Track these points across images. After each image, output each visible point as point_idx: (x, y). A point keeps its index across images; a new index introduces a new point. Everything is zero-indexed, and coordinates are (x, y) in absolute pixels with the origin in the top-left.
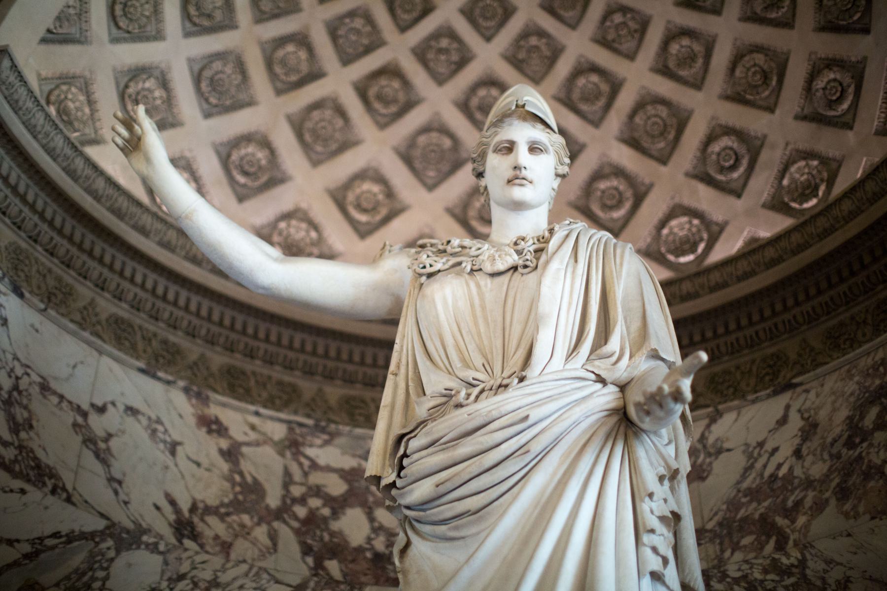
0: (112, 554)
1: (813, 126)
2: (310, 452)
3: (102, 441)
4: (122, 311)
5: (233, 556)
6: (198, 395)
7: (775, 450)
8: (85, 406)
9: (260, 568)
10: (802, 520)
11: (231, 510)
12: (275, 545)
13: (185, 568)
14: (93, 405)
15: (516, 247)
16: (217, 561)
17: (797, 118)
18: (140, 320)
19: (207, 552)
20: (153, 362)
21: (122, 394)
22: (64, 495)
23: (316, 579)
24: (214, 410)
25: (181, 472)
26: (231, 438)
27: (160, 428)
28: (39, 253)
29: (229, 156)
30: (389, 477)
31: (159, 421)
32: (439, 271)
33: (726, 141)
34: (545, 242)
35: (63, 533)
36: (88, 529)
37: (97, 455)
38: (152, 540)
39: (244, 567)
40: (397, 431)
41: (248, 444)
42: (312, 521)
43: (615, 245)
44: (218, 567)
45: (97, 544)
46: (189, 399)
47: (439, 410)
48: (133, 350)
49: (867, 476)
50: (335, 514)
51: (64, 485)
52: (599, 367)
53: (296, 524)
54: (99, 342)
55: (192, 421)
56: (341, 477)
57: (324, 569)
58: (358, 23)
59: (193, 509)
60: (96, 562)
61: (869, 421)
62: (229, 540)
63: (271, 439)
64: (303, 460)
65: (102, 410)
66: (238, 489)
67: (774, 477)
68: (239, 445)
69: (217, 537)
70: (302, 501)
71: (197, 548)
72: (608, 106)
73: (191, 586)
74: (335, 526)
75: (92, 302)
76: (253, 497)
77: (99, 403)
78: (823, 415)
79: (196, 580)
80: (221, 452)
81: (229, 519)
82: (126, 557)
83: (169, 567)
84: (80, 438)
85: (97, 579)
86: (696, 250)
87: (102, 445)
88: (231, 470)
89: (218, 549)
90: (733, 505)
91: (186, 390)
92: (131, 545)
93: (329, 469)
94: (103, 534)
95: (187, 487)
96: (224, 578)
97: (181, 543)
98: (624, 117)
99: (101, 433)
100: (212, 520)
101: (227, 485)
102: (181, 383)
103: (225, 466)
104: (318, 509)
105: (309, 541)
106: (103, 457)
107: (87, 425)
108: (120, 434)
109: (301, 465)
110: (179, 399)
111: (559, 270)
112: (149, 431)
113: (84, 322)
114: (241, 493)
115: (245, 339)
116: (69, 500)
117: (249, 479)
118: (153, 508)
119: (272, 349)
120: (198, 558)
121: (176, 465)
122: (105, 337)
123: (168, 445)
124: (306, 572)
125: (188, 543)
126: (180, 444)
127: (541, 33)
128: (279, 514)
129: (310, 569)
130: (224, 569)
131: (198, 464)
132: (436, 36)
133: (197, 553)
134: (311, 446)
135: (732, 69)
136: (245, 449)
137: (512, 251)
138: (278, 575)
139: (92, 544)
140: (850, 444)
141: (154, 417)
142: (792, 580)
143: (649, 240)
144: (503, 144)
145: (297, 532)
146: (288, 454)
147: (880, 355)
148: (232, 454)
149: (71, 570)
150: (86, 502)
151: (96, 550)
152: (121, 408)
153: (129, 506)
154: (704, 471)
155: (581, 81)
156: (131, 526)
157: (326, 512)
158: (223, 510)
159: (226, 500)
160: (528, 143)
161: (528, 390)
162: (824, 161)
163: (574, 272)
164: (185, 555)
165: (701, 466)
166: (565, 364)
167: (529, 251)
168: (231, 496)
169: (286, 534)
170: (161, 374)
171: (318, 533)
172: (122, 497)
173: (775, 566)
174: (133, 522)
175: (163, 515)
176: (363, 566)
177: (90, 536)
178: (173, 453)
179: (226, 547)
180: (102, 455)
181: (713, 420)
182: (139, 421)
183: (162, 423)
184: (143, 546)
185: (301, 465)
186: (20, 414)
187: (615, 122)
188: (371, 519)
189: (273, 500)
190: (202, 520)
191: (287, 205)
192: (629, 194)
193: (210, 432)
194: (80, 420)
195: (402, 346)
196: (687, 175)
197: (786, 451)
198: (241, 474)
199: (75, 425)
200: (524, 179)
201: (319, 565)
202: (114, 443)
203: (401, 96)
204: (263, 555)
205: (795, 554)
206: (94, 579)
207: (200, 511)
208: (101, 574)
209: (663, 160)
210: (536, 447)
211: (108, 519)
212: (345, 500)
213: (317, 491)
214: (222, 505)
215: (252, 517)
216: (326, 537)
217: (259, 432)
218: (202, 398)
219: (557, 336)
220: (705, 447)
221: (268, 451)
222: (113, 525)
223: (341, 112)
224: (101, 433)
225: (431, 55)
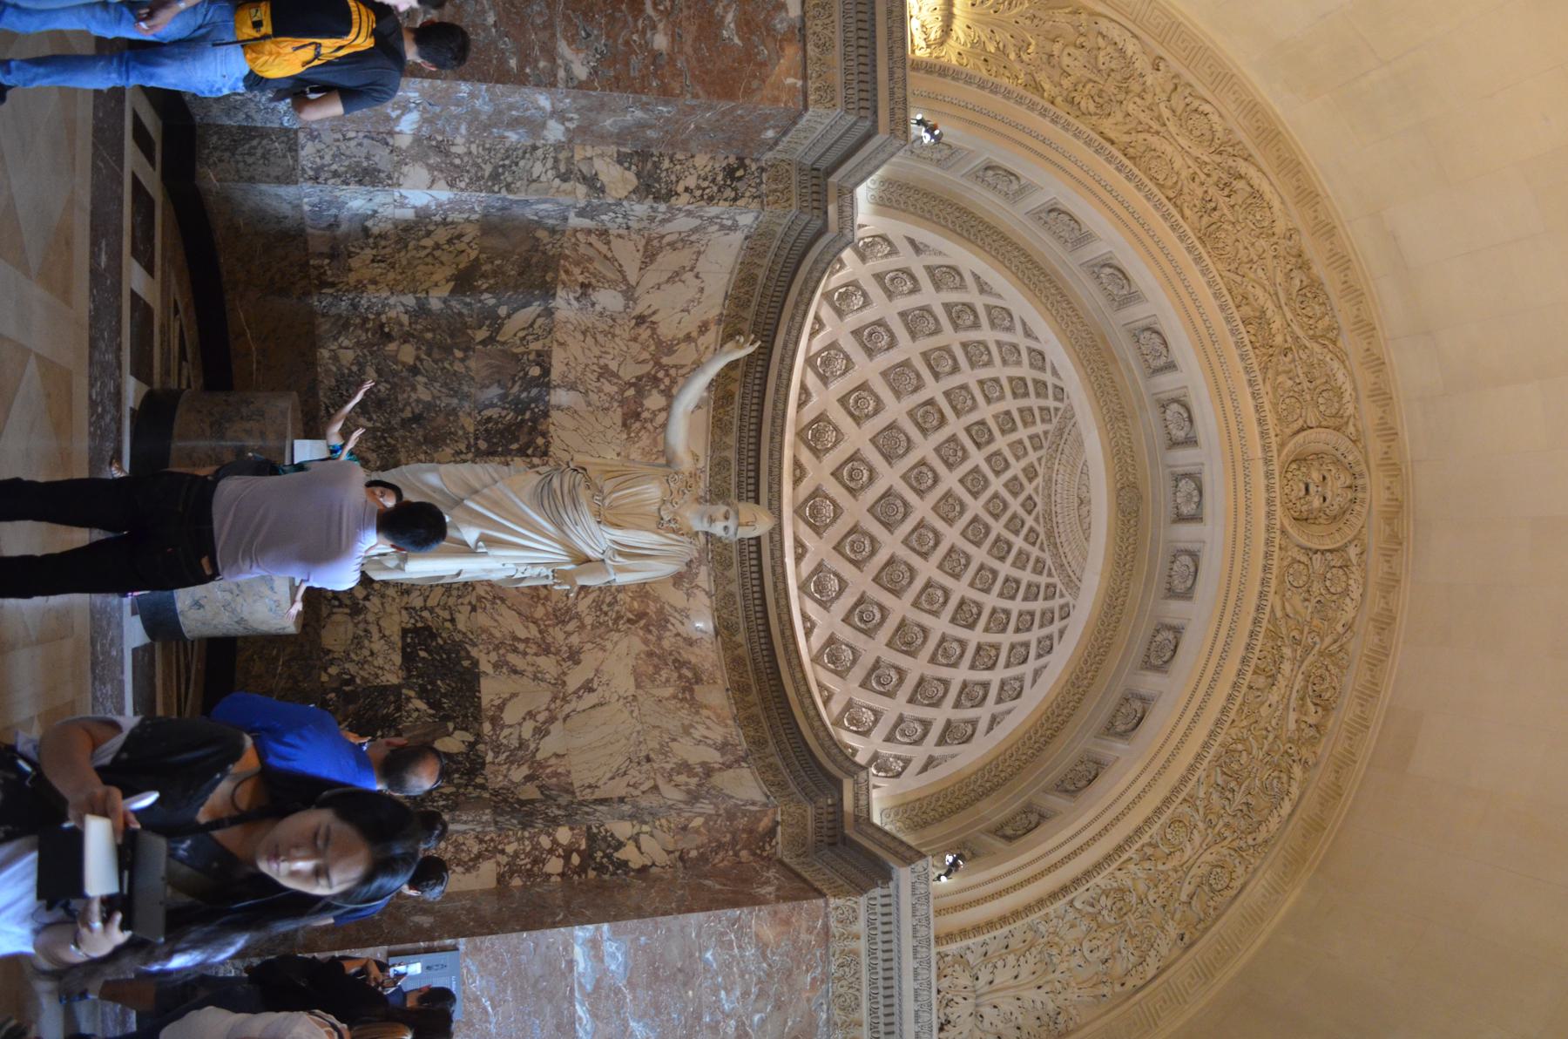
1: (870, 666)
4: (761, 279)
5: (631, 343)
6: (720, 320)
7: (683, 624)
10: (641, 633)
13: (619, 321)
16: (626, 336)
17: (879, 658)
18: (758, 289)
24: (713, 328)
28: (776, 243)
29: (880, 325)
30: (572, 466)
31: (699, 303)
33: (878, 616)
36: (629, 278)
39: (625, 349)
42: (655, 380)
48: (736, 287)
49: (656, 666)
55: (705, 318)
58: (969, 402)
61: (685, 671)
65: (697, 277)
67: (667, 621)
68: (695, 340)
72: (913, 550)
74: (655, 392)
78: (697, 650)
90: (657, 599)
91: (721, 314)
94: (628, 284)
96: (617, 339)
98: (905, 559)
99: (683, 278)
100: (649, 332)
102: (725, 312)
103: (681, 335)
106: (670, 280)
110: (715, 312)
124: (626, 379)
125: (634, 321)
127: (962, 513)
128: (658, 364)
132: (964, 449)
135: (919, 625)
138: (623, 366)
140: (675, 661)
142: (610, 623)
145: (649, 373)
147: (719, 681)
148: (688, 338)
155: (931, 535)
157: (662, 387)
162: (849, 669)
169: (647, 368)
173: (619, 617)
176: (633, 407)
177: (625, 279)
179: (635, 339)
181: (707, 593)
186: (680, 245)
187: (904, 553)
188: (660, 410)
189: (665, 360)
191: (854, 358)
192: (859, 557)
196: (864, 592)
197: (681, 629)
201: (631, 385)
203: (927, 426)
205: (624, 627)
209: (876, 580)
210: (565, 528)
218: (719, 322)
221: (695, 356)
223: (916, 390)
225: (952, 445)
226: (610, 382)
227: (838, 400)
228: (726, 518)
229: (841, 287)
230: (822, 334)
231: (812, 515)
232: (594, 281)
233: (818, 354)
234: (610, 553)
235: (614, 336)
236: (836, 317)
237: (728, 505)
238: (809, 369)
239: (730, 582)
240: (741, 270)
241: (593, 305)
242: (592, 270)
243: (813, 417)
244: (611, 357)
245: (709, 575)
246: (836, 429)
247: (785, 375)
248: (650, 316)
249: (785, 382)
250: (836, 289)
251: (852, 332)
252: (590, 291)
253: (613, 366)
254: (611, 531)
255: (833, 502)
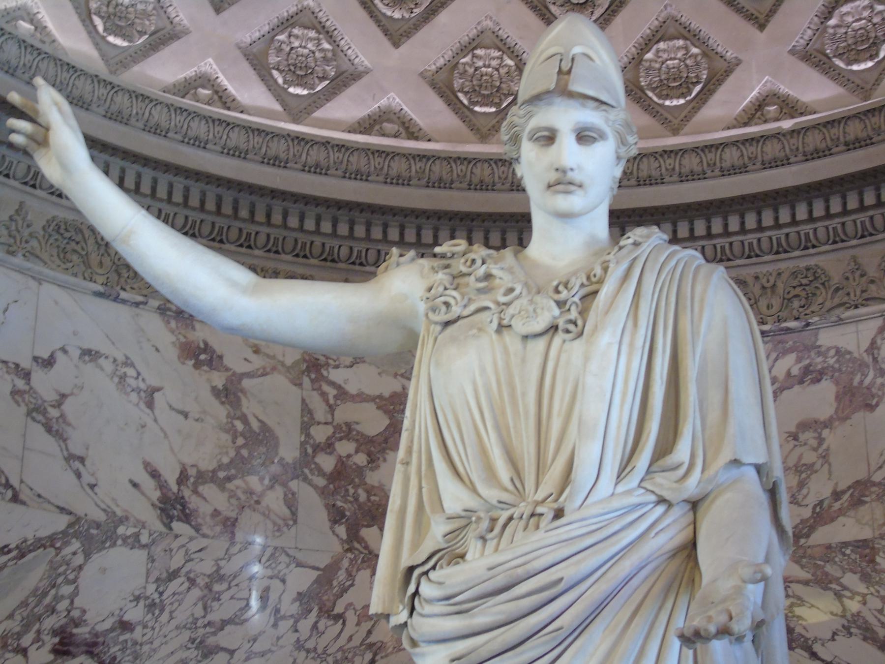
0: (79, 559)
2: (336, 375)
3: (53, 406)
8: (26, 363)
9: (276, 548)
11: (233, 472)
12: (294, 514)
13: (177, 561)
14: (36, 359)
15: (557, 297)
19: (205, 536)
20: (114, 277)
21: (75, 333)
22: (10, 493)
23: (349, 555)
25: (162, 429)
26: (227, 369)
27: (131, 372)
31: (128, 363)
32: (459, 318)
34: (597, 283)
35: (12, 546)
36: (44, 533)
37: (49, 430)
38: (131, 531)
40: (406, 561)
41: (250, 375)
43: (698, 267)
44: (221, 554)
45: (59, 549)
46: (168, 322)
47: (458, 535)
50: (373, 460)
51: (7, 480)
52: (661, 485)
53: (321, 482)
54: (38, 268)
55: (172, 353)
56: (378, 408)
57: (361, 540)
59: (182, 479)
60: (60, 575)
62: (233, 515)
63: (283, 364)
64: (326, 388)
65: (49, 363)
66: (240, 441)
69: (216, 513)
70: (328, 447)
71: (191, 532)
73: (186, 585)
74: (372, 478)
75: (21, 208)
76: (263, 449)
77: (46, 355)
79: (192, 575)
80: (215, 391)
81: (230, 486)
82: (97, 560)
83: (156, 564)
84: (23, 409)
85: (63, 597)
86: (877, 55)
87: (54, 413)
88: (228, 416)
89: (218, 529)
92: (104, 542)
93: (361, 398)
94: (65, 535)
95: (172, 449)
96: (228, 568)
97: (171, 529)
99: (50, 396)
100: (209, 490)
101: (226, 438)
103: (221, 412)
104: (349, 456)
105: (339, 504)
107: (31, 388)
108: (75, 391)
109: (324, 395)
111: (610, 344)
112: (116, 380)
113: (12, 241)
114: (244, 446)
115: (238, 224)
116: (15, 499)
117: (255, 425)
118: (129, 486)
119: (275, 233)
120: (194, 546)
121: (155, 420)
122: (45, 256)
123: (143, 394)
124: (338, 548)
125: (177, 526)
126: (158, 390)
129: (343, 542)
130: (228, 555)
131: (186, 415)
133: (191, 539)
134: (337, 367)
136: (246, 383)
137: (553, 304)
138: (300, 556)
139: (52, 551)
141: (121, 358)
143: (810, 32)
144: (540, 131)
145: (322, 492)
146: (306, 381)
149: (26, 593)
150: (39, 496)
151: (59, 558)
152: (75, 353)
153: (96, 489)
154: (873, 396)
156: (101, 517)
158: (222, 474)
159: (226, 460)
160: (575, 130)
161: (563, 533)
163: (631, 345)
164: (175, 545)
165: (868, 388)
166: (616, 484)
167: (574, 302)
168: (232, 453)
170: (123, 295)
171: (351, 491)
172: (87, 478)
174: (104, 510)
175: (143, 494)
178: (150, 405)
179: (230, 525)
180: (55, 427)
182: (102, 369)
183: (132, 365)
184: (119, 542)
185: (324, 395)
189: (289, 451)
190: (195, 492)
191: (287, 8)
193: (198, 365)
194: (20, 384)
195: (414, 421)
198: (244, 419)
199: (15, 393)
200: (570, 183)
202: (68, 407)
204: (279, 530)
206: (58, 599)
207: (192, 480)
208: (67, 590)
211: (70, 513)
212: (386, 441)
213: (347, 431)
214: (220, 467)
215: (262, 479)
216: (363, 496)
217: (268, 356)
219: (605, 447)
220: (875, 360)
221: (279, 380)
222: (78, 519)
224: (50, 396)
226: (344, 590)
227: (396, 45)
228: (549, 138)
229: (91, 29)
230: (223, 81)
231: (684, 88)
232: (50, 622)
233: (278, 93)
234: (664, 483)
235: (218, 576)
236: (175, 46)
237: (516, 140)
238: (318, 114)
239: (858, 268)
240: (30, 255)
241: (125, 626)
242: (14, 625)
243: (438, 104)
244: (276, 583)
245: (840, 322)
246: (469, 47)
247: (317, 155)
248: (162, 486)
249: (334, 156)
250: (98, 41)
251: (218, 10)
252: (82, 632)
253: (302, 579)
254: (584, 473)
255: (648, 43)
